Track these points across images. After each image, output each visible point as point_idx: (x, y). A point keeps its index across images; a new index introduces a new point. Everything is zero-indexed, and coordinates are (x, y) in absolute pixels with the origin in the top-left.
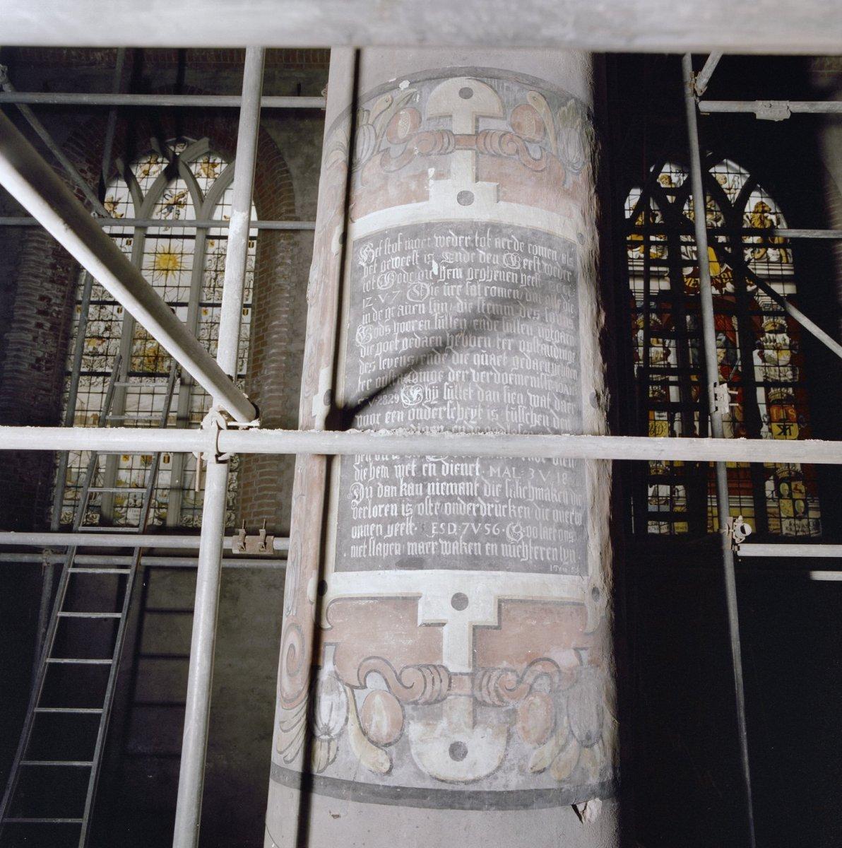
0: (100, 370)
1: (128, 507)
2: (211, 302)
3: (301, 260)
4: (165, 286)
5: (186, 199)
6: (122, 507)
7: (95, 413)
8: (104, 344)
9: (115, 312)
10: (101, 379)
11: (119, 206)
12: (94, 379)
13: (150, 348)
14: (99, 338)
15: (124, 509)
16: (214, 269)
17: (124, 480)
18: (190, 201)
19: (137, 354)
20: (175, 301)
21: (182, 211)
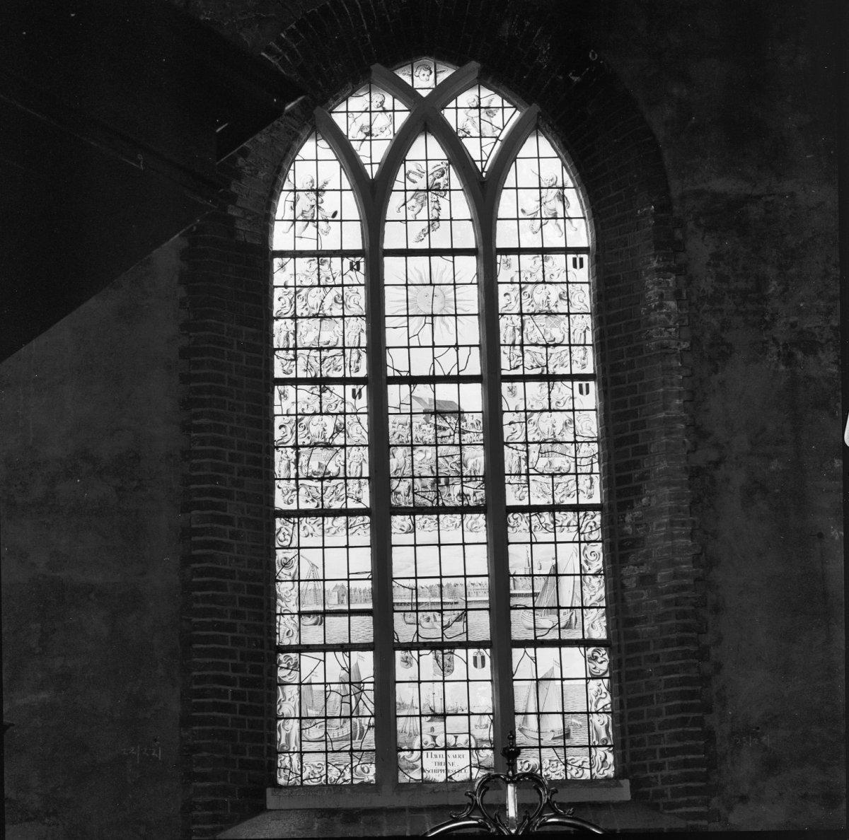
0: (337, 505)
1: (422, 750)
2: (519, 372)
3: (694, 299)
4: (433, 346)
5: (449, 179)
6: (412, 750)
7: (339, 583)
8: (338, 457)
9: (349, 397)
10: (342, 520)
11: (326, 197)
12: (329, 521)
13: (421, 462)
14: (327, 446)
15: (417, 754)
16: (517, 310)
17: (408, 702)
18: (456, 182)
19: (399, 474)
20: (454, 373)
21: (444, 203)
